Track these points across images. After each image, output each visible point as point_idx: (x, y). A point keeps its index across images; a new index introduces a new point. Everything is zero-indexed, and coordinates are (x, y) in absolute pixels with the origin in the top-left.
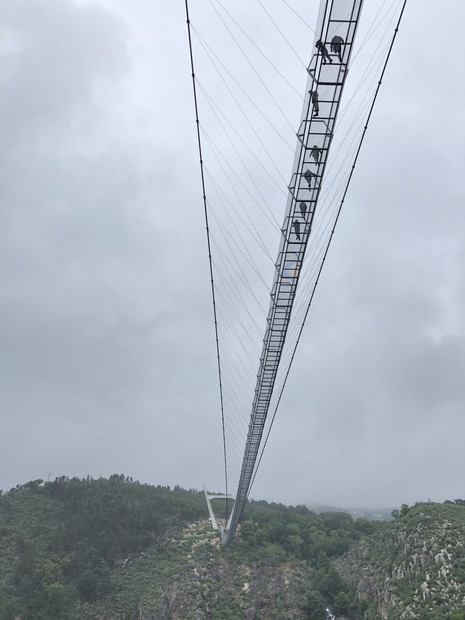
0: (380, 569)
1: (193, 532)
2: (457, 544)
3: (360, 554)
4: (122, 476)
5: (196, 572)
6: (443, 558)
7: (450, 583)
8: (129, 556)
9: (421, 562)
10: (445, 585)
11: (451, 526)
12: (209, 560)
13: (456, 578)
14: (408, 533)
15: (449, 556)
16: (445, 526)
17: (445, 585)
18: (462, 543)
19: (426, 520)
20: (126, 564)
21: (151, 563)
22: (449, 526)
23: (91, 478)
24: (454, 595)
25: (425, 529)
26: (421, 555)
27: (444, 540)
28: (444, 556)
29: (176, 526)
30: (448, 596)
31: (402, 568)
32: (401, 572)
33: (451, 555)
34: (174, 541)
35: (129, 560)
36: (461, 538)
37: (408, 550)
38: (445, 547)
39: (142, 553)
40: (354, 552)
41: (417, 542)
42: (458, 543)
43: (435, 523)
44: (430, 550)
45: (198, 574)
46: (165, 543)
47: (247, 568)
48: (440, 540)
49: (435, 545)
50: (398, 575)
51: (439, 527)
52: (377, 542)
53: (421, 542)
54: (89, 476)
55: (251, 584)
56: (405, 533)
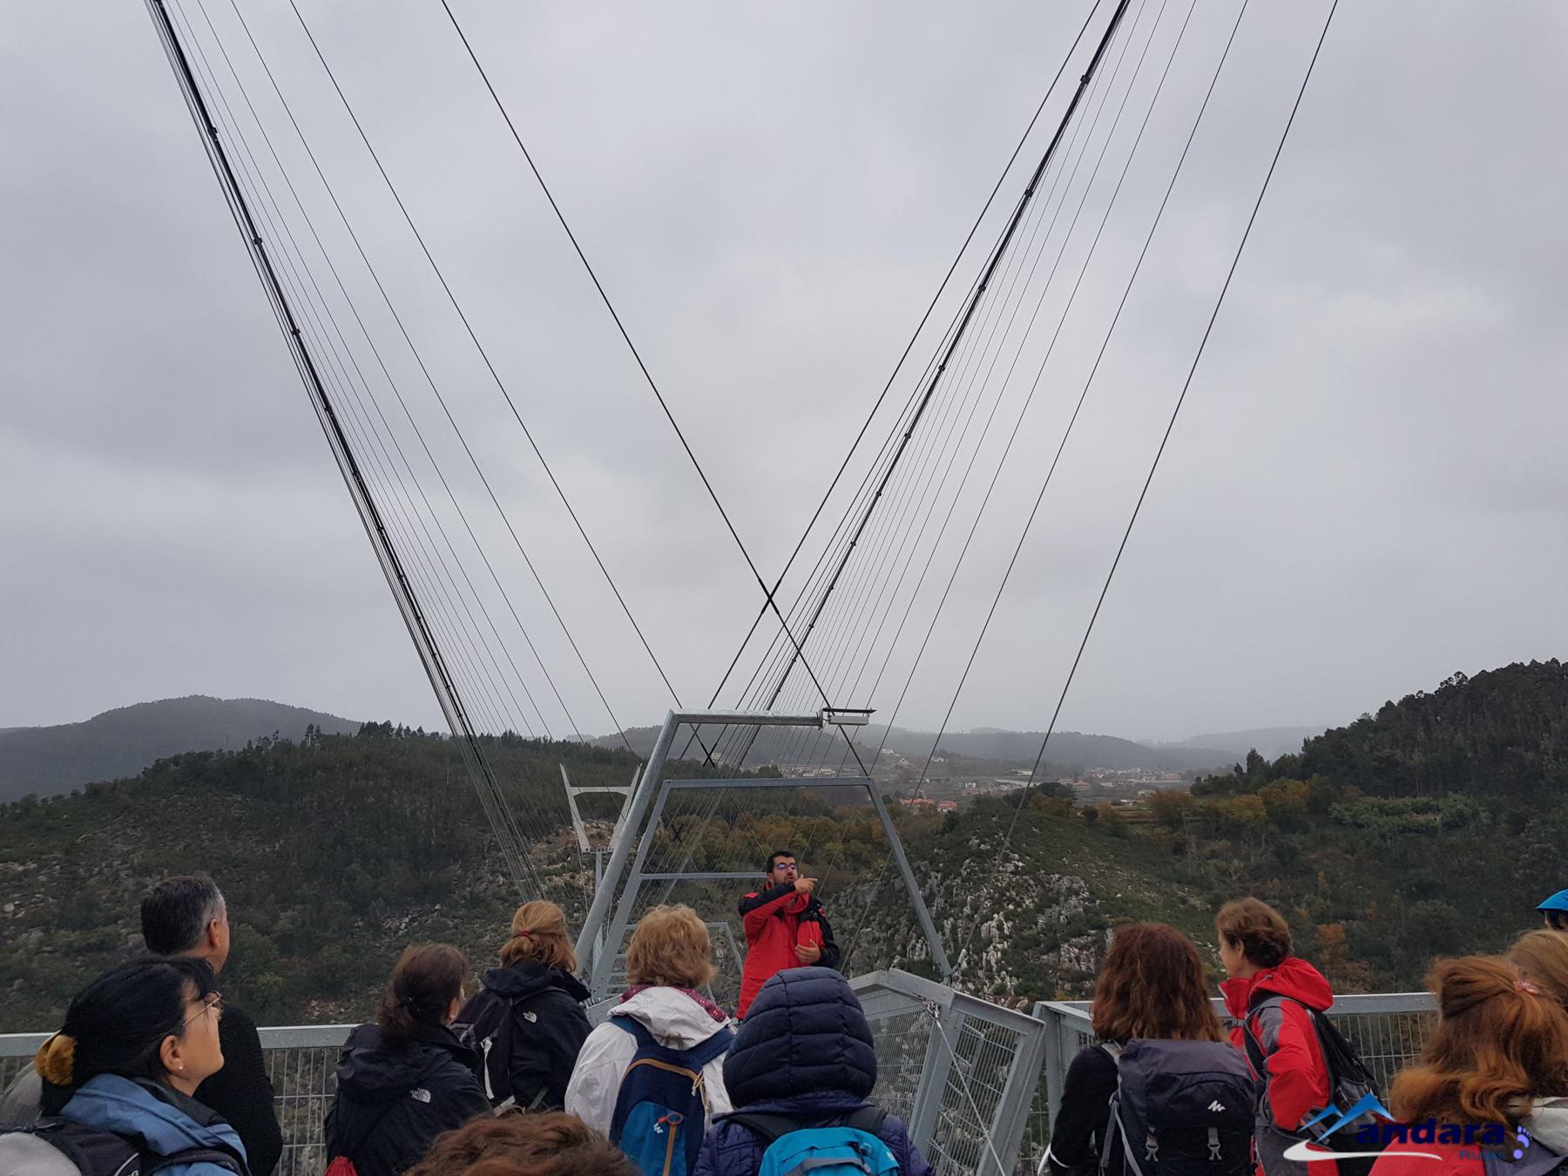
0: (891, 934)
3: (861, 898)
6: (995, 932)
7: (999, 976)
8: (411, 912)
9: (957, 934)
10: (991, 979)
11: (1022, 867)
13: (1010, 969)
14: (944, 878)
15: (1005, 927)
16: (1011, 867)
17: (991, 979)
18: (1033, 901)
20: (406, 928)
21: (456, 927)
23: (318, 731)
24: (1003, 1000)
26: (960, 921)
27: (1004, 895)
28: (997, 925)
31: (924, 942)
32: (922, 950)
33: (1010, 924)
34: (501, 879)
36: (1034, 891)
37: (939, 909)
38: (1003, 908)
40: (851, 894)
41: (956, 896)
43: (995, 860)
44: (976, 913)
46: (484, 885)
48: (996, 895)
50: (917, 954)
51: (1001, 868)
52: (895, 878)
53: (964, 897)
54: (313, 727)
56: (939, 875)
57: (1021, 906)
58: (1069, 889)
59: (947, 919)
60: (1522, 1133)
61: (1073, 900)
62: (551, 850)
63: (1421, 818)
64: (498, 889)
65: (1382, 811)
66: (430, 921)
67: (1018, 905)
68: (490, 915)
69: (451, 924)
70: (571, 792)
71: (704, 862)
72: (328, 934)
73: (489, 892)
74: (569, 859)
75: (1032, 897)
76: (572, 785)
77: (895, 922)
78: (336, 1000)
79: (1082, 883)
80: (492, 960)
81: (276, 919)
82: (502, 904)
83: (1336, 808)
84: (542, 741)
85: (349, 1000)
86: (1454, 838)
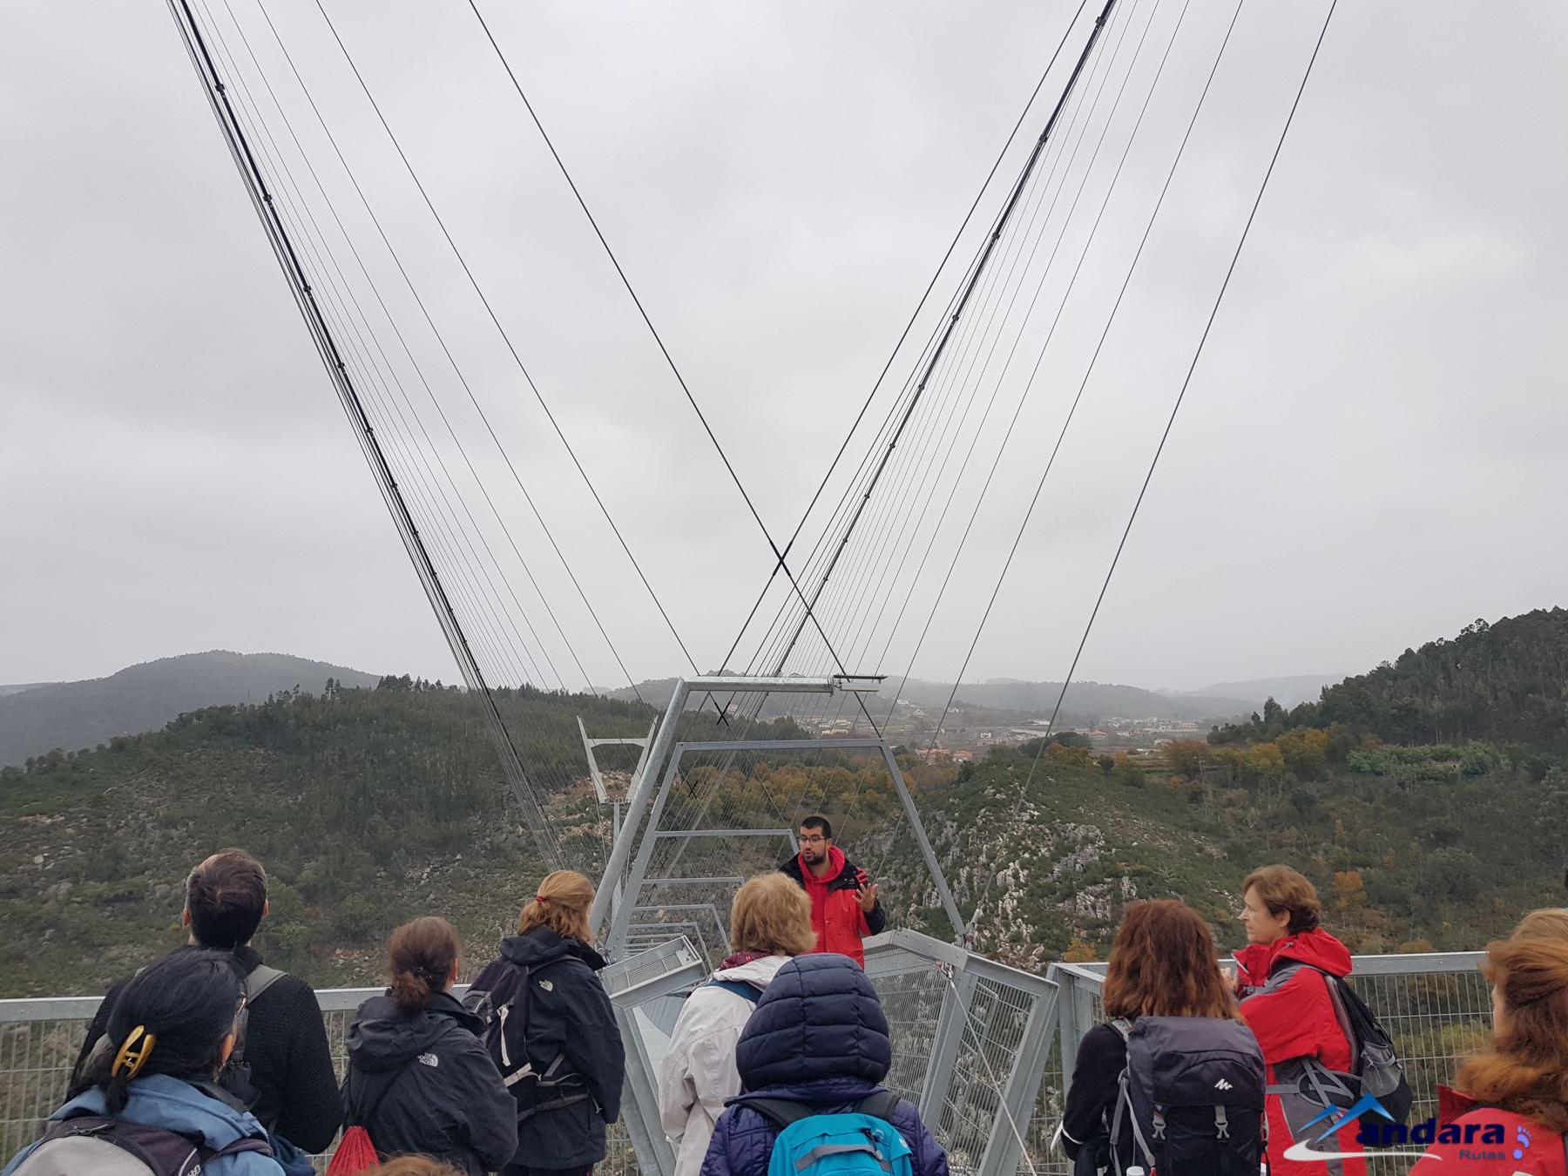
0: (907, 882)
2: (1040, 851)
3: (876, 847)
4: (406, 678)
6: (1011, 880)
7: (1015, 923)
8: (432, 862)
10: (1007, 926)
11: (1038, 816)
12: (591, 866)
13: (1026, 916)
14: (960, 828)
15: (1021, 875)
16: (1026, 817)
17: (1007, 926)
18: (1049, 850)
20: (427, 877)
21: (477, 876)
22: (1032, 816)
23: (338, 685)
24: (1019, 947)
25: (992, 821)
26: (976, 870)
27: (1020, 844)
30: (1008, 948)
32: (938, 898)
33: (1026, 872)
34: (521, 830)
35: (434, 870)
36: (1049, 840)
37: (955, 858)
39: (458, 857)
41: (972, 844)
43: (1011, 809)
46: (504, 836)
53: (980, 846)
54: (333, 681)
56: (955, 824)
58: (1085, 838)
59: (963, 867)
60: (1522, 1133)
61: (1089, 849)
63: (1440, 766)
64: (518, 839)
65: (1401, 758)
66: (451, 870)
67: (1034, 853)
69: (472, 874)
70: (590, 744)
71: (721, 812)
72: (351, 884)
74: (587, 809)
75: (1048, 845)
76: (592, 736)
77: (911, 871)
78: (361, 948)
79: (1098, 831)
80: (512, 909)
81: (300, 869)
83: (1355, 757)
84: (559, 694)
85: (373, 949)
86: (1474, 785)
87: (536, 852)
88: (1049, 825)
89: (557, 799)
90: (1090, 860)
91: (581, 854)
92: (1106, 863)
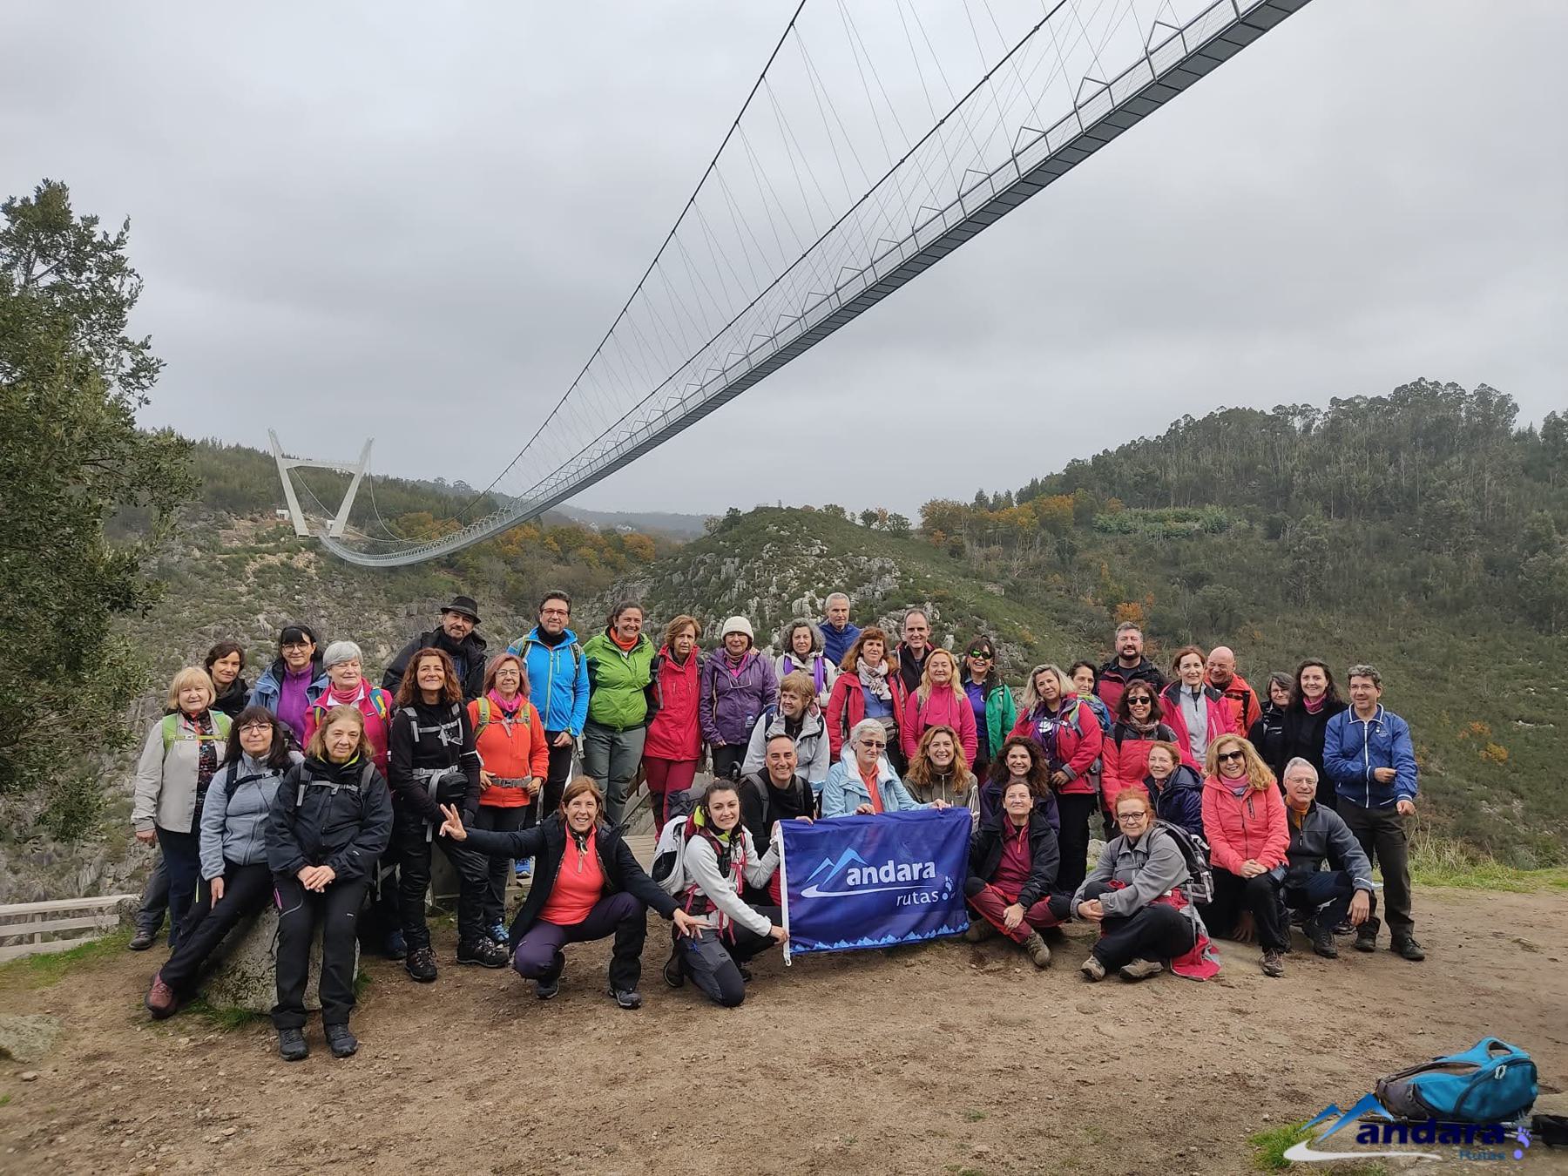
1: (247, 538)
5: (262, 620)
6: (808, 608)
12: (294, 599)
19: (781, 539)
22: (822, 551)
29: (200, 522)
34: (197, 553)
38: (812, 587)
40: (619, 592)
42: (837, 582)
45: (269, 627)
46: (176, 558)
47: (385, 617)
49: (795, 583)
51: (804, 552)
55: (395, 647)
56: (737, 560)
57: (830, 585)
58: (881, 568)
59: (752, 598)
61: (887, 579)
62: (259, 528)
63: (1181, 525)
65: (1146, 519)
68: (186, 590)
73: (184, 566)
74: (283, 539)
75: (841, 577)
80: (195, 637)
82: (202, 579)
83: (1102, 518)
84: (210, 443)
86: (1219, 539)
87: (220, 579)
88: (840, 558)
89: (243, 525)
90: (888, 588)
91: (280, 585)
92: (907, 590)
